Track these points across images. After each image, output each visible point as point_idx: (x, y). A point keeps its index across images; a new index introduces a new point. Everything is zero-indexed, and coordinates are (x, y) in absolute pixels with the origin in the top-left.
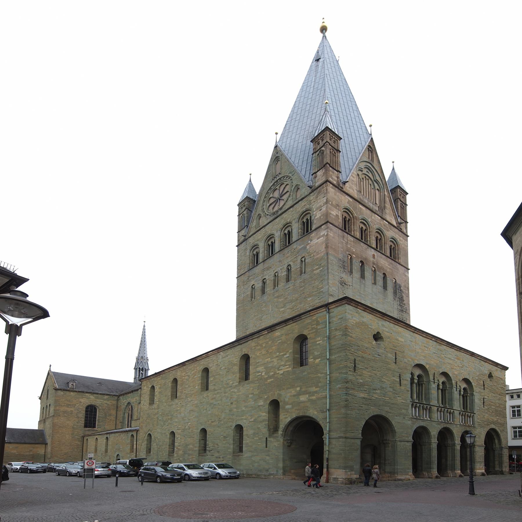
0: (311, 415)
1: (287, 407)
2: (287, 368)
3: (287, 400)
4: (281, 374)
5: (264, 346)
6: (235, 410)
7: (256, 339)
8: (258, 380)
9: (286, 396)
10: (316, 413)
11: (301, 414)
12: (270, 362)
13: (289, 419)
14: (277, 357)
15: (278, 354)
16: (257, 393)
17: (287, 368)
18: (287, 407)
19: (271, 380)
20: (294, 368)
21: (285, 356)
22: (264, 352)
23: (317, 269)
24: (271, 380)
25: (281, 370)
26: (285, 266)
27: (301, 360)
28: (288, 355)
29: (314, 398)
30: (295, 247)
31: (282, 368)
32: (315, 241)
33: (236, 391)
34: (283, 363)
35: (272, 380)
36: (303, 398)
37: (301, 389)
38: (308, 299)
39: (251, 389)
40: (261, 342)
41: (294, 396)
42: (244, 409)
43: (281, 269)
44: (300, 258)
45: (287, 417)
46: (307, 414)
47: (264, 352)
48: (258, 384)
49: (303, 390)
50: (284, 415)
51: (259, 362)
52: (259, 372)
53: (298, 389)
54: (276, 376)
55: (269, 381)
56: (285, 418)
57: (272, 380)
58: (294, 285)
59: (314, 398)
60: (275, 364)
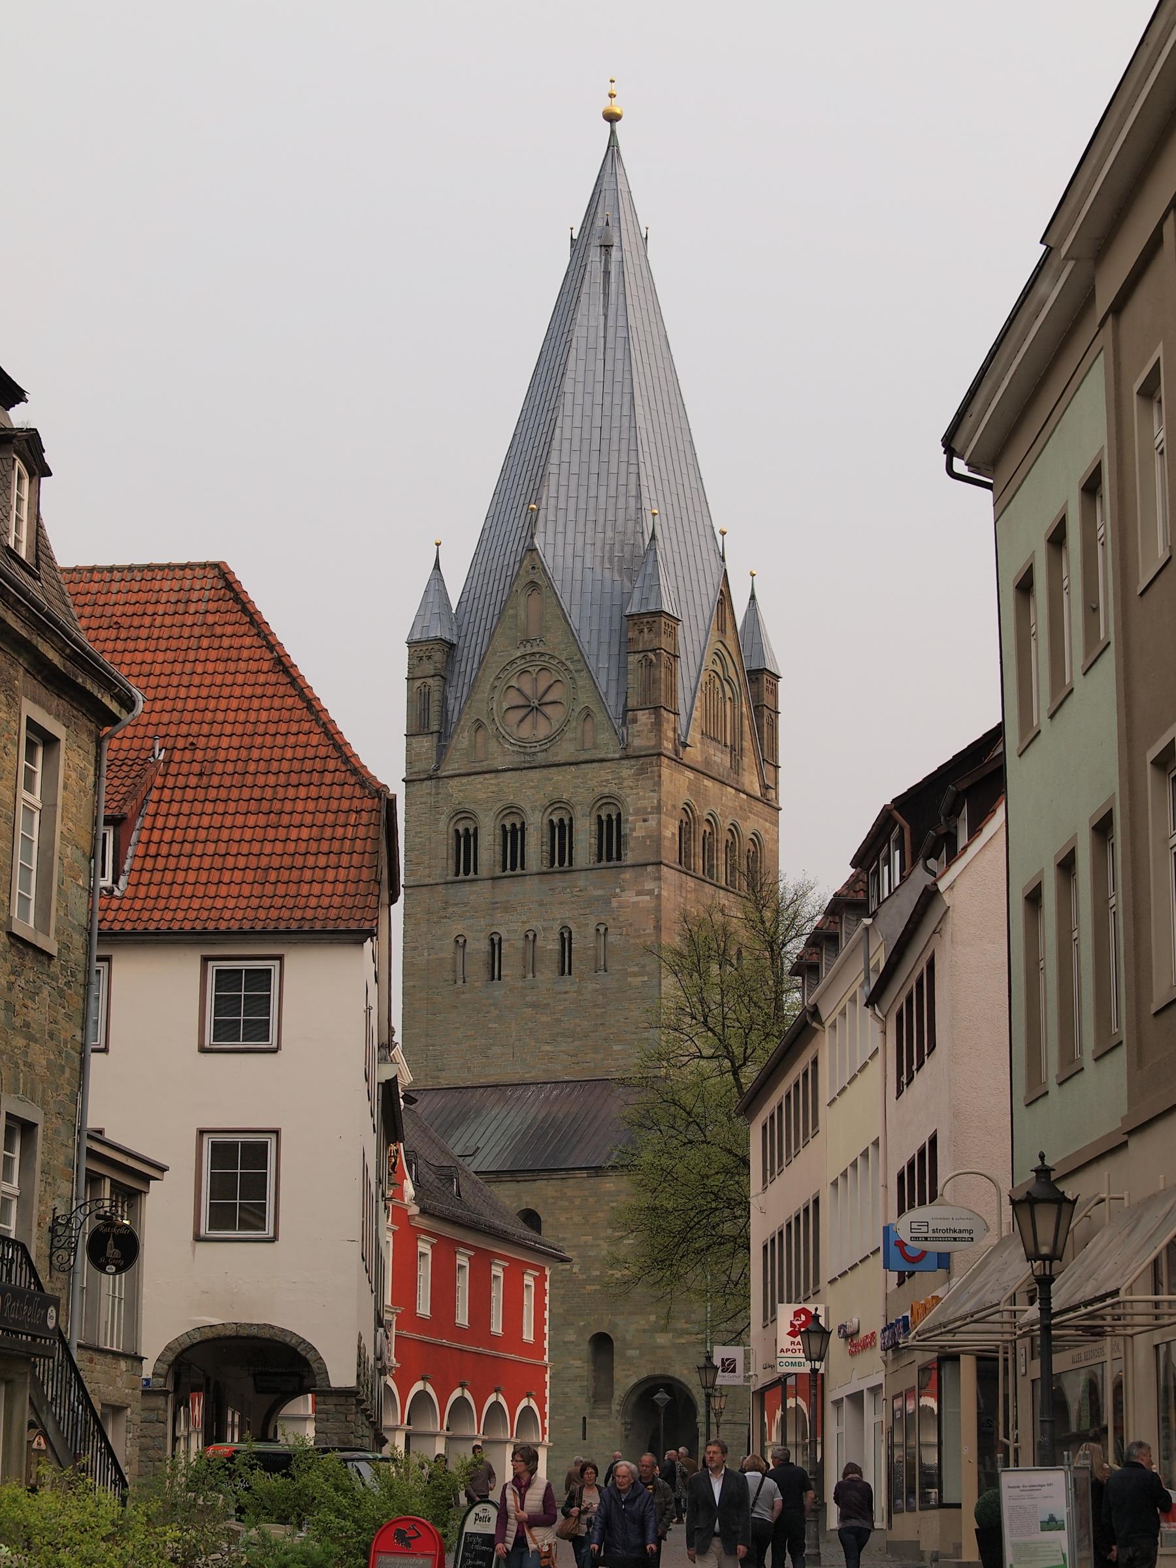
1: (630, 1353)
3: (628, 1337)
5: (577, 1202)
7: (559, 1182)
18: (630, 1353)
19: (593, 1287)
22: (576, 1219)
23: (635, 975)
24: (593, 1287)
26: (557, 928)
30: (581, 883)
32: (630, 897)
35: (598, 1287)
38: (615, 1048)
40: (569, 1192)
43: (545, 929)
44: (593, 923)
56: (627, 1376)
58: (579, 992)
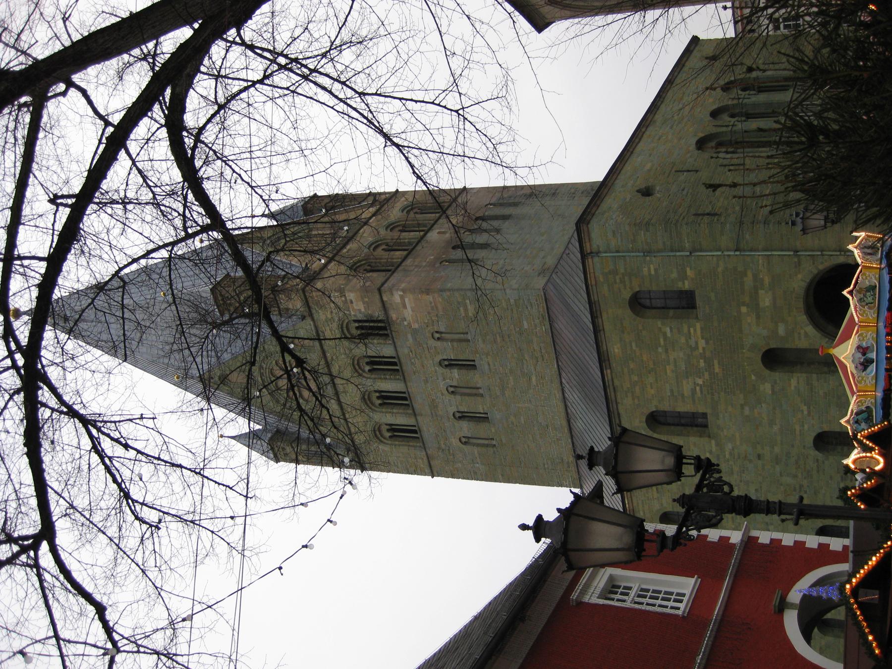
0: (804, 285)
2: (695, 330)
3: (765, 333)
4: (707, 343)
6: (777, 450)
8: (713, 395)
9: (756, 333)
10: (800, 276)
11: (801, 305)
12: (676, 366)
13: (810, 329)
14: (666, 351)
15: (660, 350)
16: (741, 396)
17: (695, 330)
20: (697, 318)
21: (669, 335)
25: (697, 343)
27: (685, 302)
28: (668, 330)
29: (767, 280)
31: (692, 342)
33: (730, 446)
34: (683, 340)
35: (716, 362)
36: (766, 300)
37: (744, 304)
39: (730, 409)
41: (758, 317)
42: (776, 428)
45: (806, 333)
46: (802, 292)
47: (651, 379)
48: (722, 394)
49: (747, 299)
50: (800, 339)
51: (672, 391)
52: (694, 391)
53: (744, 309)
54: (708, 354)
55: (717, 370)
57: (716, 362)
59: (767, 280)
60: (681, 355)
